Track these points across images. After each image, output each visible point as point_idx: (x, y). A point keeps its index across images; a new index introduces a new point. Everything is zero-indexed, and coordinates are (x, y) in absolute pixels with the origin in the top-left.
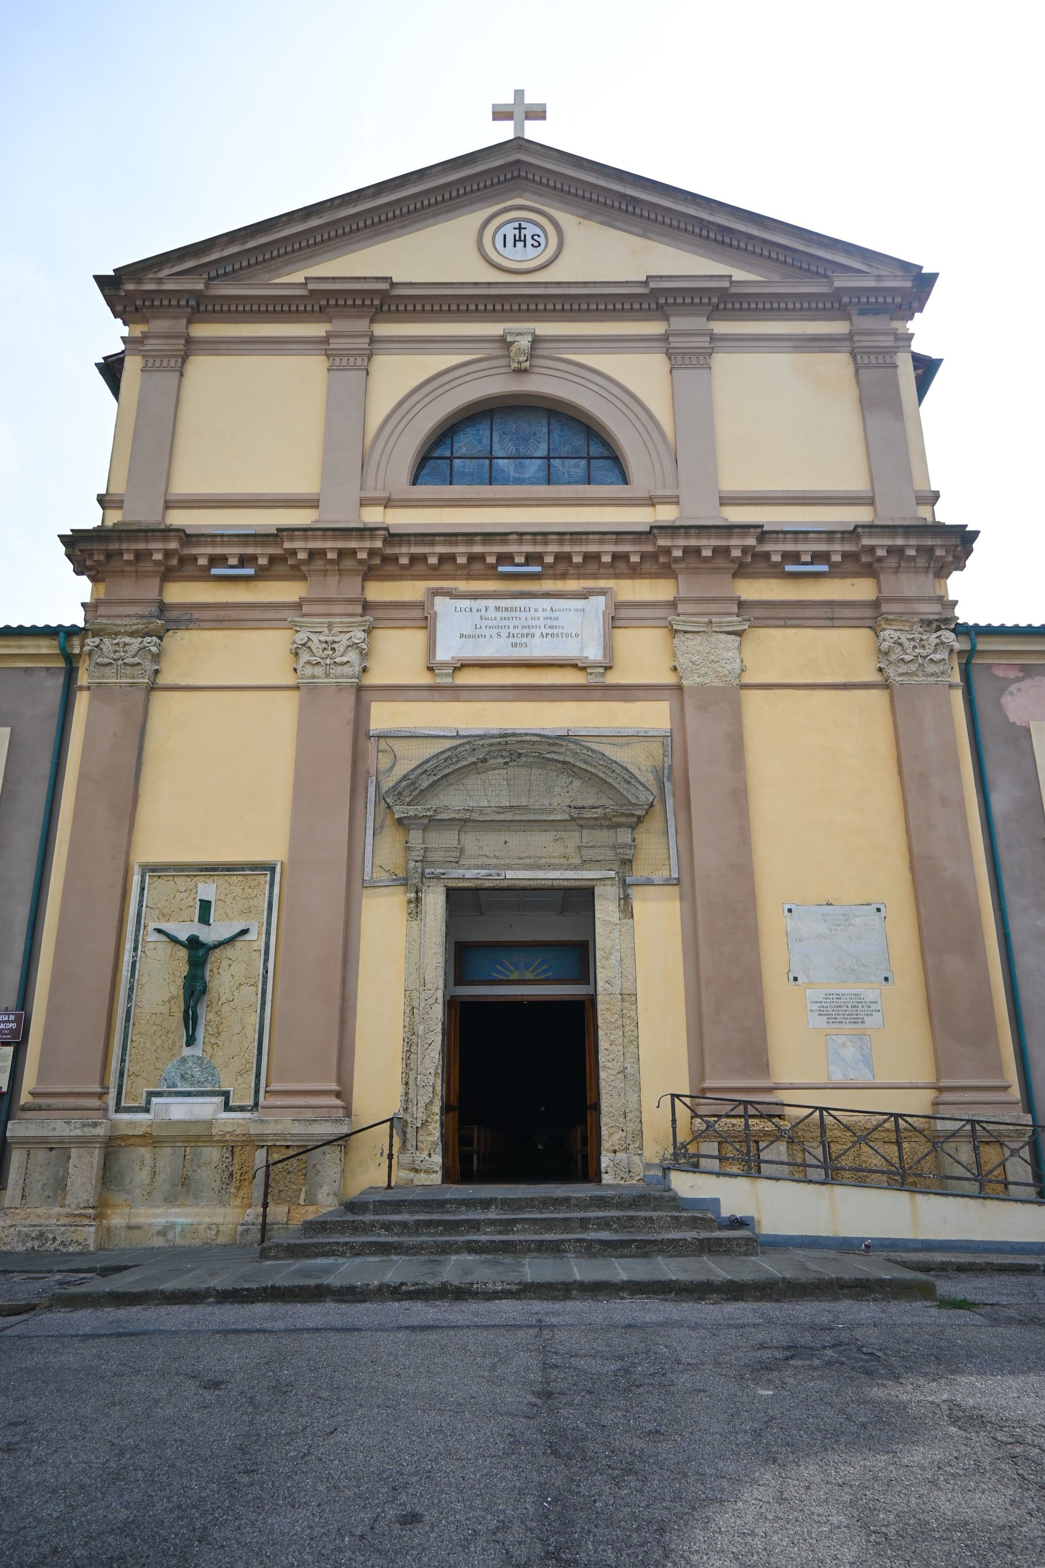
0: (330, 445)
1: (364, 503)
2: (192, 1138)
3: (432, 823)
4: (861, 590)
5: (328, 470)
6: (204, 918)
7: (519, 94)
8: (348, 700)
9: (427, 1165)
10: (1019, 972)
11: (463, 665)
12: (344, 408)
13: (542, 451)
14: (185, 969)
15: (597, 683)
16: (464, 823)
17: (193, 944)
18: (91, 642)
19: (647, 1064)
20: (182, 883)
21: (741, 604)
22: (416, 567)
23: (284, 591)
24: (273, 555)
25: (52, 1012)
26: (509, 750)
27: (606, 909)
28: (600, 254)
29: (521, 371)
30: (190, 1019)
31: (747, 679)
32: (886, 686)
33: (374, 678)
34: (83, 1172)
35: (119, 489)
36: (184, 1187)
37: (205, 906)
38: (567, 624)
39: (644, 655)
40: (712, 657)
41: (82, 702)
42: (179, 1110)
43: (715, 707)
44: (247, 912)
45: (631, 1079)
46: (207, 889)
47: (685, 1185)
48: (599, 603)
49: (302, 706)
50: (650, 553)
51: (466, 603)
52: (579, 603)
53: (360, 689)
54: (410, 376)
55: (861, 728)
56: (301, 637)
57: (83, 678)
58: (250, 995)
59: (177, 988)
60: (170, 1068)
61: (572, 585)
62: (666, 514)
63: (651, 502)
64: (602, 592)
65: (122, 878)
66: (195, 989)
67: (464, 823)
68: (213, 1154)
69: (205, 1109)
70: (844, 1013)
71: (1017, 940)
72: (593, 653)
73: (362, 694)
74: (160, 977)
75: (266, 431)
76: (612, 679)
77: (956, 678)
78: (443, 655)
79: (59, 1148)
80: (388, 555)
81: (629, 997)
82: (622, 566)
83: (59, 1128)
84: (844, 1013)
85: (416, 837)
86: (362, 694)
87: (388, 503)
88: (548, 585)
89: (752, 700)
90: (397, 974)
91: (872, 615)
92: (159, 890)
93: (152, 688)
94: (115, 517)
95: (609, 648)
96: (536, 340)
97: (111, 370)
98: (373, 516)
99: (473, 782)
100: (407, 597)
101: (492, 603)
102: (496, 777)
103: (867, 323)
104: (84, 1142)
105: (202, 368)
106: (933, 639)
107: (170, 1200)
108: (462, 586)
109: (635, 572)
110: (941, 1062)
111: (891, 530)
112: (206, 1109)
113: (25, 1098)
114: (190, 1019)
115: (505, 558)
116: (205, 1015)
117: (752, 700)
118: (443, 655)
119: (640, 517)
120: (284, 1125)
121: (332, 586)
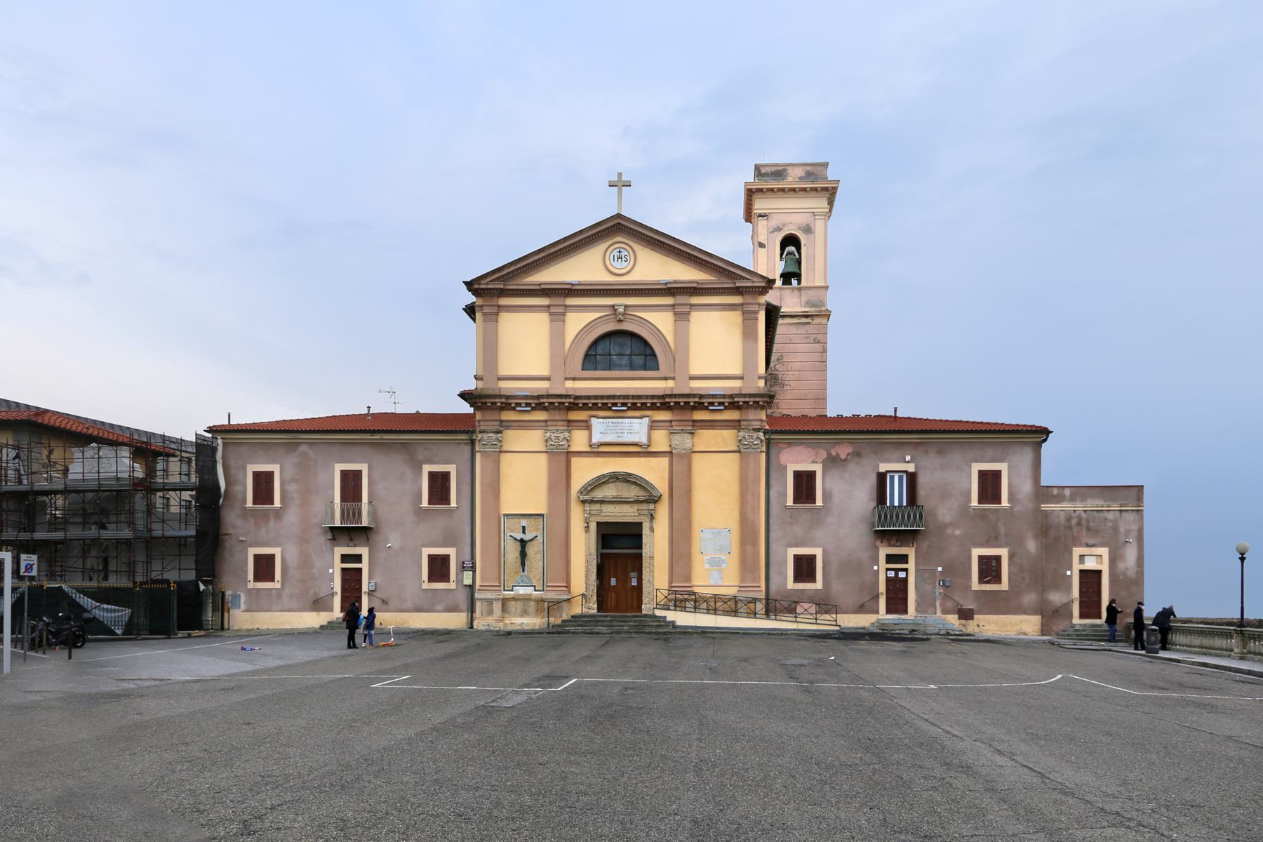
2: (526, 599)
3: (592, 502)
4: (733, 415)
5: (553, 365)
7: (620, 175)
8: (563, 458)
9: (593, 608)
12: (557, 337)
15: (644, 451)
16: (602, 502)
17: (522, 541)
18: (480, 436)
19: (657, 576)
21: (694, 421)
22: (585, 407)
23: (541, 416)
24: (538, 403)
26: (616, 478)
27: (646, 531)
29: (620, 321)
30: (523, 564)
32: (739, 452)
34: (497, 607)
35: (480, 373)
36: (525, 613)
38: (635, 429)
39: (661, 440)
40: (683, 442)
41: (478, 456)
42: (522, 591)
43: (681, 462)
44: (537, 530)
45: (651, 582)
46: (524, 522)
47: (658, 613)
48: (646, 420)
49: (550, 461)
50: (663, 403)
54: (580, 322)
56: (548, 435)
57: (477, 449)
58: (539, 556)
59: (517, 554)
60: (518, 578)
63: (666, 379)
65: (497, 519)
66: (523, 555)
67: (602, 502)
68: (532, 604)
69: (529, 591)
70: (716, 563)
71: (771, 539)
72: (644, 440)
73: (569, 454)
74: (512, 552)
75: (530, 348)
77: (764, 449)
79: (490, 602)
81: (652, 558)
82: (654, 407)
83: (489, 595)
84: (716, 563)
85: (587, 507)
86: (569, 454)
87: (574, 379)
88: (630, 413)
89: (697, 458)
90: (582, 550)
91: (736, 425)
92: (510, 522)
94: (481, 385)
95: (649, 438)
96: (626, 306)
97: (471, 310)
99: (605, 488)
100: (581, 418)
102: (611, 485)
103: (749, 299)
104: (497, 600)
105: (505, 318)
106: (755, 435)
107: (521, 616)
108: (601, 413)
109: (658, 409)
110: (743, 579)
111: (745, 395)
112: (529, 591)
113: (477, 587)
114: (523, 564)
115: (615, 404)
116: (527, 563)
117: (696, 457)
118: (595, 440)
121: (557, 416)
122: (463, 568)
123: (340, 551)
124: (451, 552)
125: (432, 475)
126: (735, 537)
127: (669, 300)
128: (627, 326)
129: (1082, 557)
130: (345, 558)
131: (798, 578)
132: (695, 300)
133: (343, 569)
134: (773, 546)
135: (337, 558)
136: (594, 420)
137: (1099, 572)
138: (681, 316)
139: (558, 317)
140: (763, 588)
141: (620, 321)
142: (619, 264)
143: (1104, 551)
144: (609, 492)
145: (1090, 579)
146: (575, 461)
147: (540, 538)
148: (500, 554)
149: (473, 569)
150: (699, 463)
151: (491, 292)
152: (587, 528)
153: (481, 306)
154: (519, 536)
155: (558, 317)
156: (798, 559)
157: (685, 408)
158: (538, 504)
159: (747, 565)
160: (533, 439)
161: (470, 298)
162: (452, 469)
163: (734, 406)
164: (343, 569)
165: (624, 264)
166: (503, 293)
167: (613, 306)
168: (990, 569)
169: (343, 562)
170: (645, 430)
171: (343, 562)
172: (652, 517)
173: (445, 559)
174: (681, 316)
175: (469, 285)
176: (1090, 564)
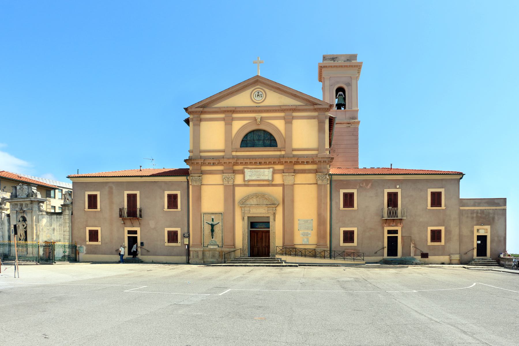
0: (226, 140)
1: (232, 152)
4: (314, 167)
6: (213, 221)
10: (332, 229)
11: (249, 181)
13: (262, 139)
14: (211, 228)
15: (270, 184)
20: (209, 215)
23: (220, 168)
25: (193, 234)
27: (271, 220)
28: (273, 99)
30: (212, 235)
31: (295, 183)
32: (317, 184)
33: (237, 182)
37: (213, 219)
38: (266, 174)
39: (278, 179)
40: (289, 179)
41: (191, 187)
45: (274, 243)
46: (213, 217)
48: (271, 170)
51: (249, 170)
52: (268, 170)
53: (233, 185)
54: (240, 126)
55: (312, 191)
57: (190, 183)
58: (220, 232)
59: (210, 231)
61: (267, 166)
62: (283, 153)
63: (280, 151)
64: (271, 168)
65: (200, 215)
66: (212, 231)
69: (216, 247)
71: (333, 224)
72: (270, 178)
73: (234, 186)
76: (274, 183)
77: (329, 182)
78: (246, 179)
80: (237, 161)
82: (274, 163)
86: (234, 186)
87: (236, 152)
89: (296, 187)
91: (316, 171)
92: (206, 217)
93: (202, 185)
94: (191, 154)
97: (187, 121)
98: (234, 154)
101: (254, 170)
105: (203, 124)
109: (277, 164)
112: (216, 247)
113: (191, 245)
114: (212, 235)
118: (246, 179)
119: (278, 153)
120: (226, 250)
122: (184, 236)
123: (127, 229)
124: (179, 230)
125: (169, 196)
126: (315, 224)
127: (282, 114)
128: (263, 127)
129: (478, 230)
130: (129, 232)
131: (345, 241)
132: (295, 114)
133: (129, 237)
134: (334, 226)
135: (126, 232)
136: (246, 170)
137: (485, 237)
138: (288, 122)
139: (228, 123)
140: (328, 245)
141: (259, 124)
142: (258, 98)
143: (488, 227)
144: (254, 201)
145: (482, 239)
146: (237, 189)
147: (220, 224)
148: (202, 230)
149: (189, 237)
150: (297, 188)
151: (196, 113)
152: (243, 219)
153: (192, 119)
154: (211, 222)
155: (228, 123)
156: (345, 233)
157: (292, 163)
158: (219, 207)
159: (321, 236)
160: (217, 179)
161: (187, 116)
162: (178, 193)
163: (313, 163)
164: (129, 237)
165: (260, 98)
166: (202, 113)
167: (255, 118)
168: (436, 236)
169: (128, 233)
170: (271, 174)
171: (128, 233)
172: (274, 214)
173: (176, 233)
174: (288, 122)
175: (186, 109)
176: (482, 233)
